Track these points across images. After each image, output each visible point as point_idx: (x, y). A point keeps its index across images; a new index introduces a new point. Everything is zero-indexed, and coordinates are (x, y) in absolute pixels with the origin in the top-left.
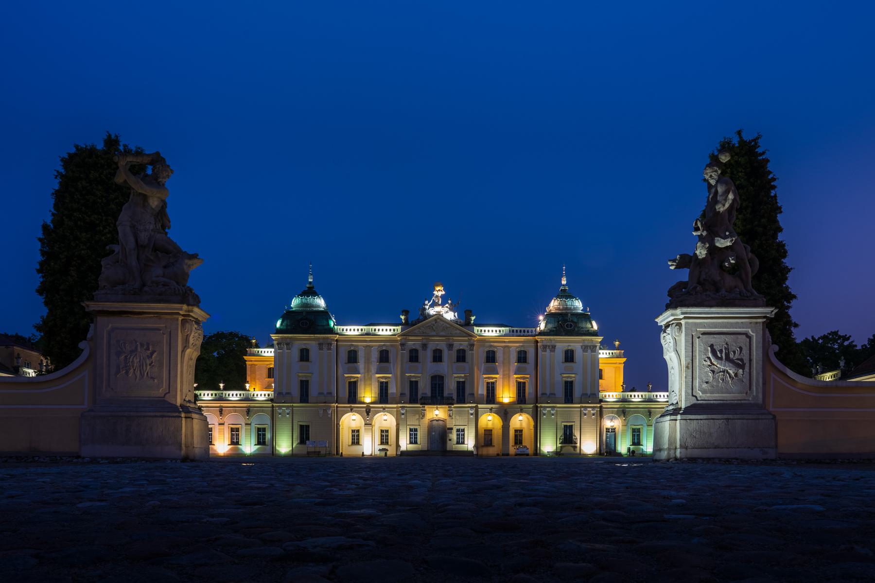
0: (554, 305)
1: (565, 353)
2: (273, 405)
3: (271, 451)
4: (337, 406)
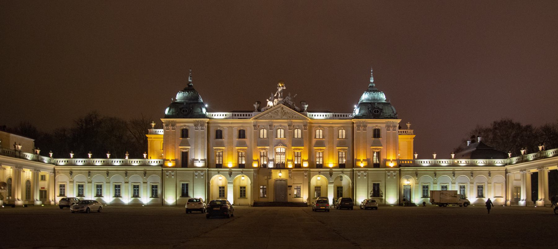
0: (365, 97)
1: (374, 131)
2: (162, 169)
3: (162, 202)
4: (208, 170)
